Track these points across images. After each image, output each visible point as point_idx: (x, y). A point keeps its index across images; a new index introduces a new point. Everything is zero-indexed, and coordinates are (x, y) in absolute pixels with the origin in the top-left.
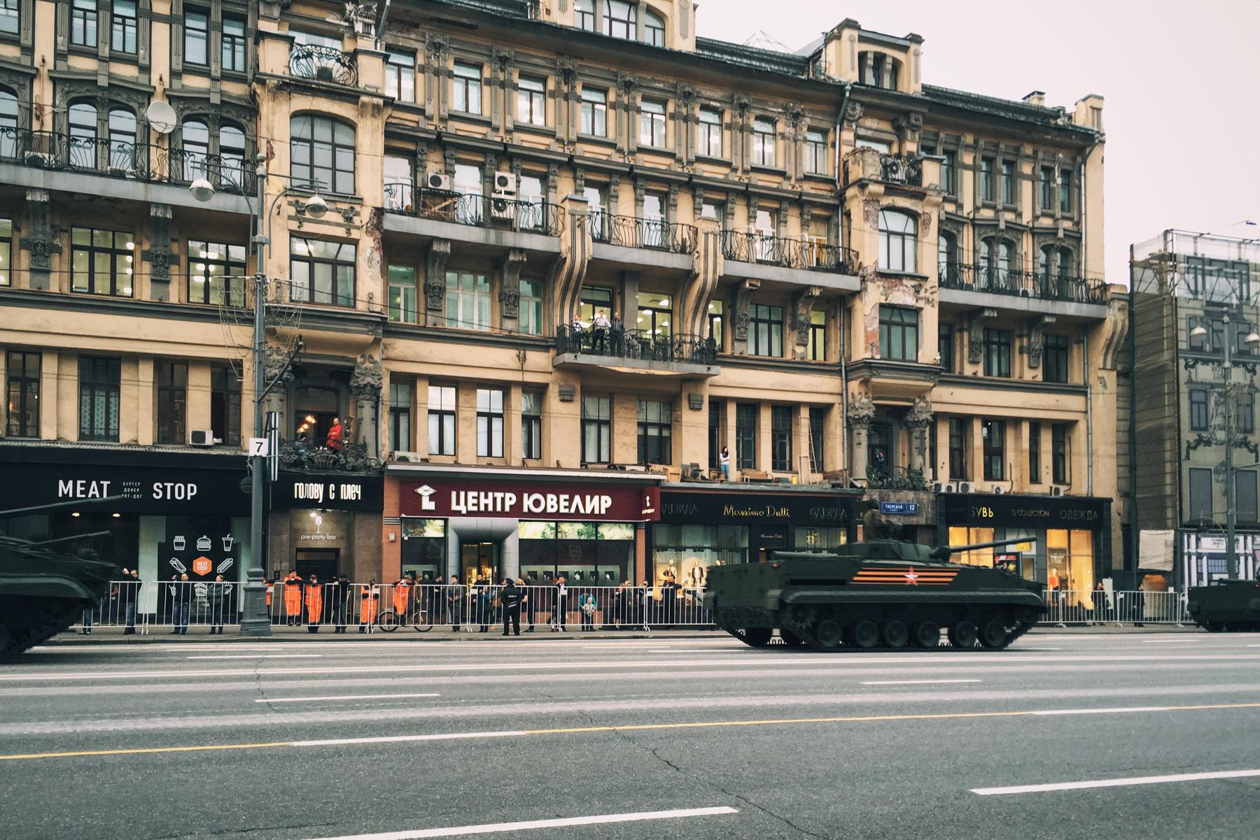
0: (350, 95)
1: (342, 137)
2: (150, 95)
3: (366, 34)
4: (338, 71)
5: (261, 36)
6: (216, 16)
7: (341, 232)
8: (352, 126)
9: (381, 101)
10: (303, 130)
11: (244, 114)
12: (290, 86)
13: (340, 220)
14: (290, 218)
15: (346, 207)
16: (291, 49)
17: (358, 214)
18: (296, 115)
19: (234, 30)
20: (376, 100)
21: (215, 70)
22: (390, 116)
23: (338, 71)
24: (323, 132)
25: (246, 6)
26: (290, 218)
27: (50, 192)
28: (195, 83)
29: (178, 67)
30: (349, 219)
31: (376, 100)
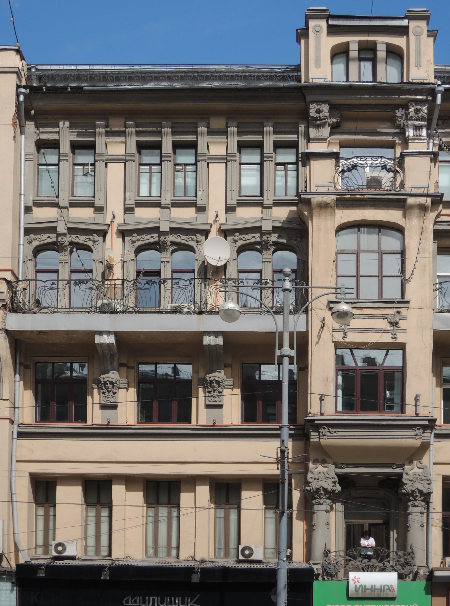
0: (398, 203)
1: (390, 242)
2: (206, 233)
3: (418, 137)
4: (386, 178)
5: (307, 158)
6: (269, 147)
7: (387, 338)
8: (400, 230)
9: (429, 200)
10: (349, 239)
11: (295, 235)
12: (345, 201)
13: (383, 324)
14: (334, 330)
15: (391, 312)
16: (337, 165)
17: (405, 317)
18: (341, 228)
19: (288, 157)
20: (422, 200)
21: (268, 200)
22: (438, 215)
23: (386, 178)
24: (369, 239)
25: (297, 133)
26: (334, 330)
27: (117, 334)
28: (248, 215)
29: (232, 202)
30: (394, 324)
31: (422, 200)
